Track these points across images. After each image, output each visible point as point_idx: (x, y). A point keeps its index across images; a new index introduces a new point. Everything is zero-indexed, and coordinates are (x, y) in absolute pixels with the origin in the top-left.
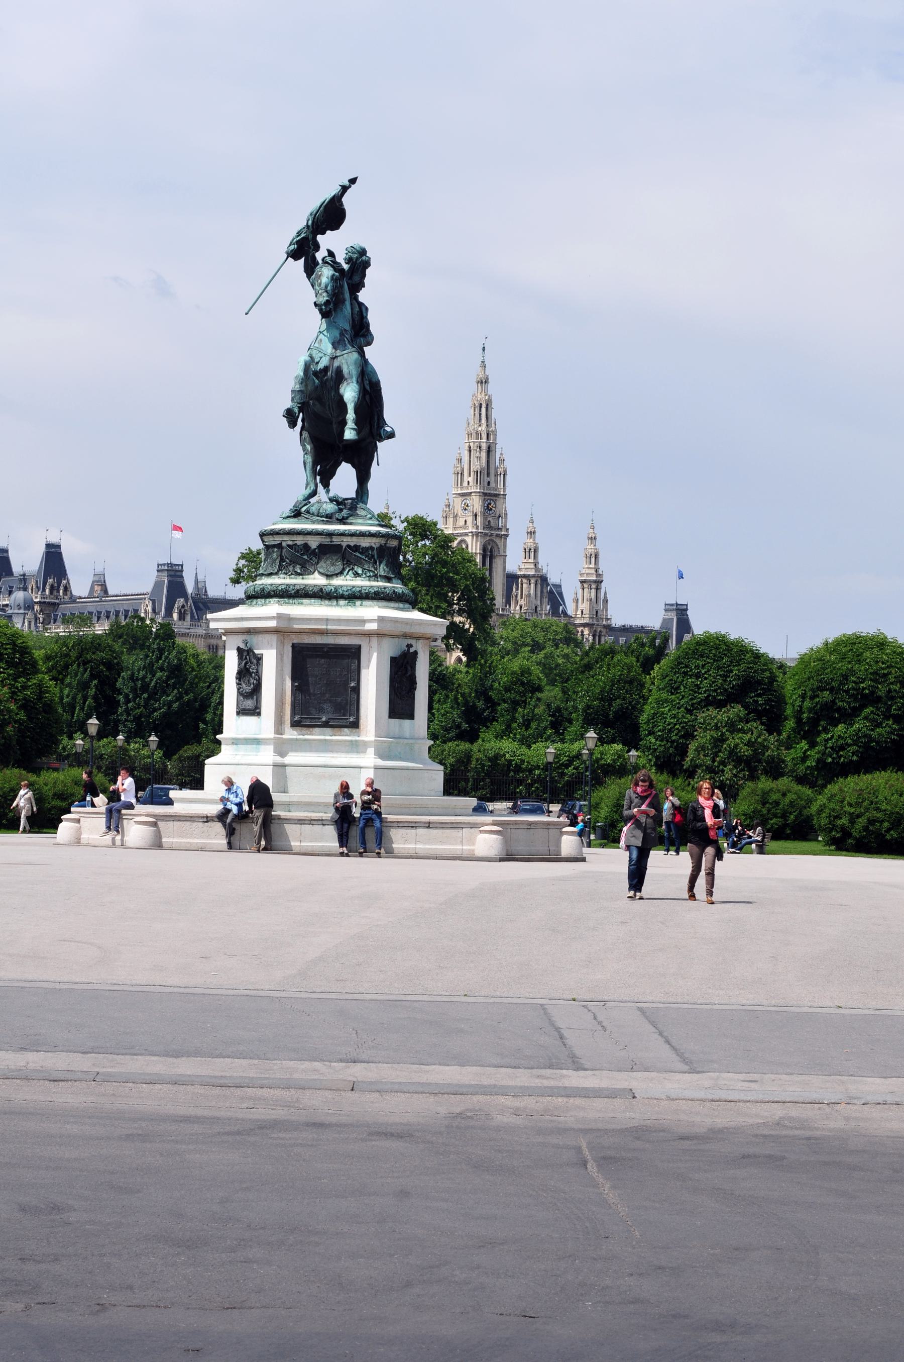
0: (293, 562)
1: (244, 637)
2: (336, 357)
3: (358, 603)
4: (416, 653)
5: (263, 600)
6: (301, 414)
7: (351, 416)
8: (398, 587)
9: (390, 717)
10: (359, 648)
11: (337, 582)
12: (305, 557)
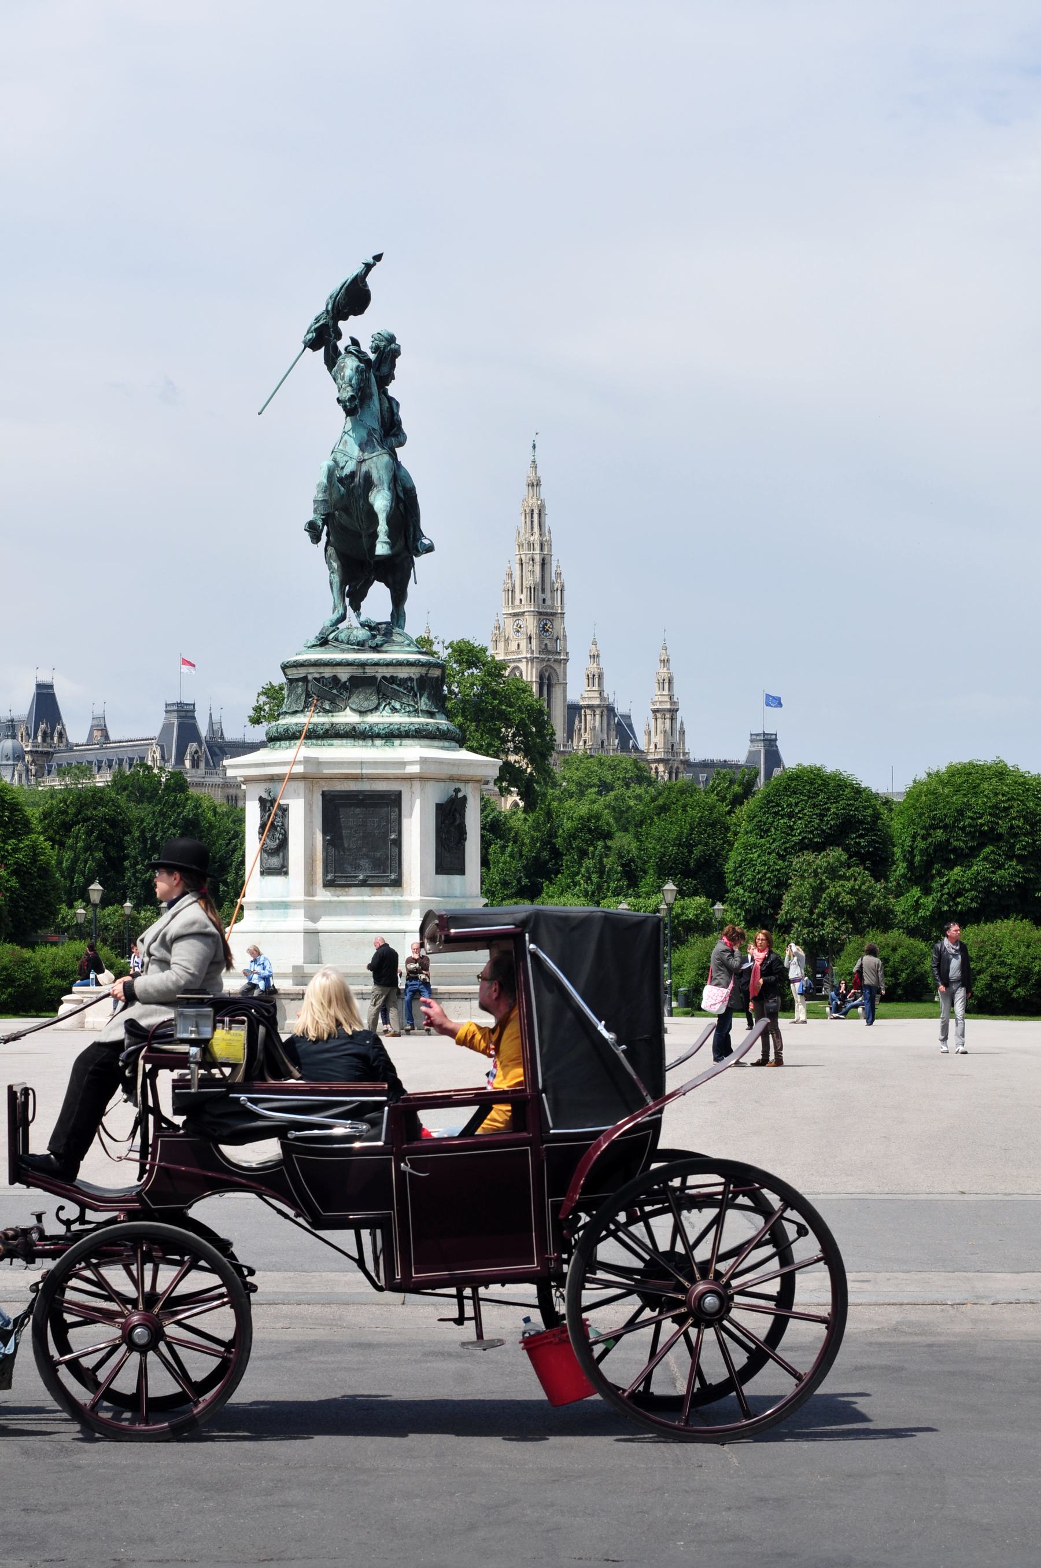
0: (321, 698)
1: (267, 785)
2: (364, 460)
3: (397, 742)
4: (465, 798)
5: (287, 742)
6: (325, 527)
7: (382, 527)
8: (442, 722)
9: (437, 873)
10: (399, 794)
11: (372, 719)
12: (335, 691)
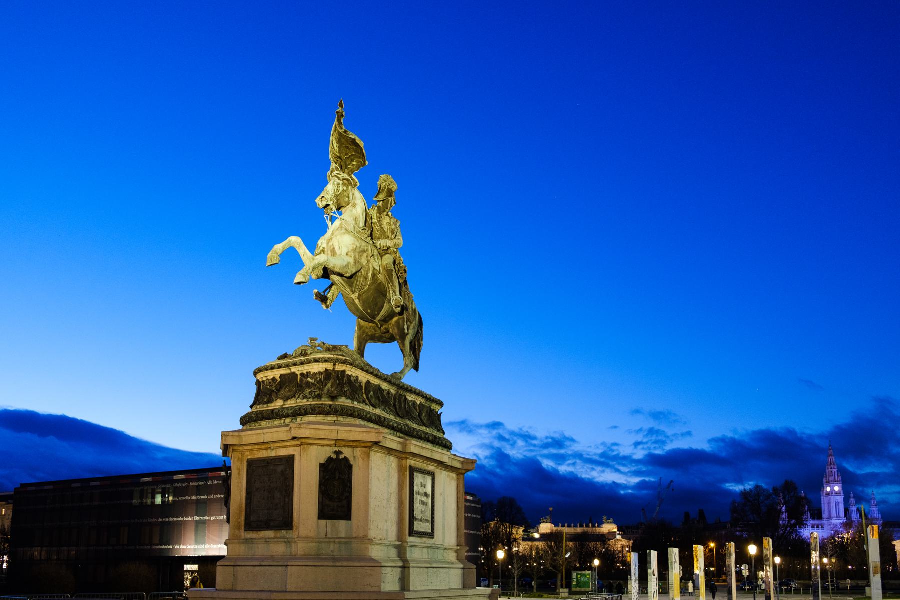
0: (265, 395)
11: (291, 403)
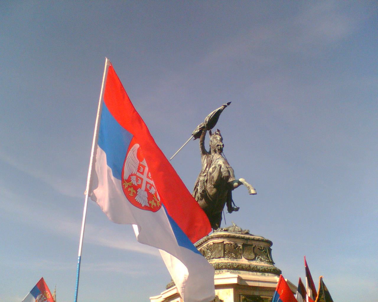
3: (266, 274)
11: (254, 263)
